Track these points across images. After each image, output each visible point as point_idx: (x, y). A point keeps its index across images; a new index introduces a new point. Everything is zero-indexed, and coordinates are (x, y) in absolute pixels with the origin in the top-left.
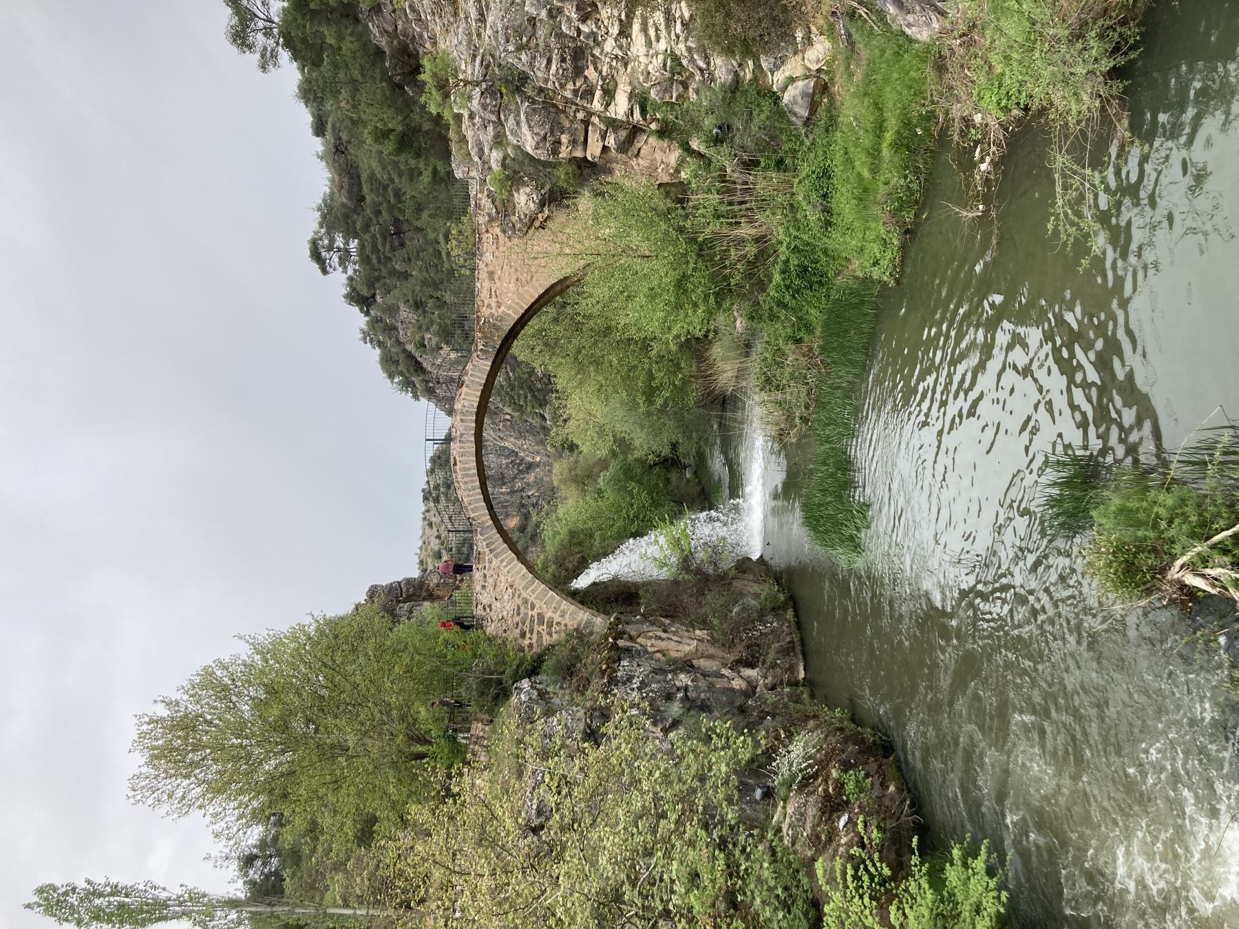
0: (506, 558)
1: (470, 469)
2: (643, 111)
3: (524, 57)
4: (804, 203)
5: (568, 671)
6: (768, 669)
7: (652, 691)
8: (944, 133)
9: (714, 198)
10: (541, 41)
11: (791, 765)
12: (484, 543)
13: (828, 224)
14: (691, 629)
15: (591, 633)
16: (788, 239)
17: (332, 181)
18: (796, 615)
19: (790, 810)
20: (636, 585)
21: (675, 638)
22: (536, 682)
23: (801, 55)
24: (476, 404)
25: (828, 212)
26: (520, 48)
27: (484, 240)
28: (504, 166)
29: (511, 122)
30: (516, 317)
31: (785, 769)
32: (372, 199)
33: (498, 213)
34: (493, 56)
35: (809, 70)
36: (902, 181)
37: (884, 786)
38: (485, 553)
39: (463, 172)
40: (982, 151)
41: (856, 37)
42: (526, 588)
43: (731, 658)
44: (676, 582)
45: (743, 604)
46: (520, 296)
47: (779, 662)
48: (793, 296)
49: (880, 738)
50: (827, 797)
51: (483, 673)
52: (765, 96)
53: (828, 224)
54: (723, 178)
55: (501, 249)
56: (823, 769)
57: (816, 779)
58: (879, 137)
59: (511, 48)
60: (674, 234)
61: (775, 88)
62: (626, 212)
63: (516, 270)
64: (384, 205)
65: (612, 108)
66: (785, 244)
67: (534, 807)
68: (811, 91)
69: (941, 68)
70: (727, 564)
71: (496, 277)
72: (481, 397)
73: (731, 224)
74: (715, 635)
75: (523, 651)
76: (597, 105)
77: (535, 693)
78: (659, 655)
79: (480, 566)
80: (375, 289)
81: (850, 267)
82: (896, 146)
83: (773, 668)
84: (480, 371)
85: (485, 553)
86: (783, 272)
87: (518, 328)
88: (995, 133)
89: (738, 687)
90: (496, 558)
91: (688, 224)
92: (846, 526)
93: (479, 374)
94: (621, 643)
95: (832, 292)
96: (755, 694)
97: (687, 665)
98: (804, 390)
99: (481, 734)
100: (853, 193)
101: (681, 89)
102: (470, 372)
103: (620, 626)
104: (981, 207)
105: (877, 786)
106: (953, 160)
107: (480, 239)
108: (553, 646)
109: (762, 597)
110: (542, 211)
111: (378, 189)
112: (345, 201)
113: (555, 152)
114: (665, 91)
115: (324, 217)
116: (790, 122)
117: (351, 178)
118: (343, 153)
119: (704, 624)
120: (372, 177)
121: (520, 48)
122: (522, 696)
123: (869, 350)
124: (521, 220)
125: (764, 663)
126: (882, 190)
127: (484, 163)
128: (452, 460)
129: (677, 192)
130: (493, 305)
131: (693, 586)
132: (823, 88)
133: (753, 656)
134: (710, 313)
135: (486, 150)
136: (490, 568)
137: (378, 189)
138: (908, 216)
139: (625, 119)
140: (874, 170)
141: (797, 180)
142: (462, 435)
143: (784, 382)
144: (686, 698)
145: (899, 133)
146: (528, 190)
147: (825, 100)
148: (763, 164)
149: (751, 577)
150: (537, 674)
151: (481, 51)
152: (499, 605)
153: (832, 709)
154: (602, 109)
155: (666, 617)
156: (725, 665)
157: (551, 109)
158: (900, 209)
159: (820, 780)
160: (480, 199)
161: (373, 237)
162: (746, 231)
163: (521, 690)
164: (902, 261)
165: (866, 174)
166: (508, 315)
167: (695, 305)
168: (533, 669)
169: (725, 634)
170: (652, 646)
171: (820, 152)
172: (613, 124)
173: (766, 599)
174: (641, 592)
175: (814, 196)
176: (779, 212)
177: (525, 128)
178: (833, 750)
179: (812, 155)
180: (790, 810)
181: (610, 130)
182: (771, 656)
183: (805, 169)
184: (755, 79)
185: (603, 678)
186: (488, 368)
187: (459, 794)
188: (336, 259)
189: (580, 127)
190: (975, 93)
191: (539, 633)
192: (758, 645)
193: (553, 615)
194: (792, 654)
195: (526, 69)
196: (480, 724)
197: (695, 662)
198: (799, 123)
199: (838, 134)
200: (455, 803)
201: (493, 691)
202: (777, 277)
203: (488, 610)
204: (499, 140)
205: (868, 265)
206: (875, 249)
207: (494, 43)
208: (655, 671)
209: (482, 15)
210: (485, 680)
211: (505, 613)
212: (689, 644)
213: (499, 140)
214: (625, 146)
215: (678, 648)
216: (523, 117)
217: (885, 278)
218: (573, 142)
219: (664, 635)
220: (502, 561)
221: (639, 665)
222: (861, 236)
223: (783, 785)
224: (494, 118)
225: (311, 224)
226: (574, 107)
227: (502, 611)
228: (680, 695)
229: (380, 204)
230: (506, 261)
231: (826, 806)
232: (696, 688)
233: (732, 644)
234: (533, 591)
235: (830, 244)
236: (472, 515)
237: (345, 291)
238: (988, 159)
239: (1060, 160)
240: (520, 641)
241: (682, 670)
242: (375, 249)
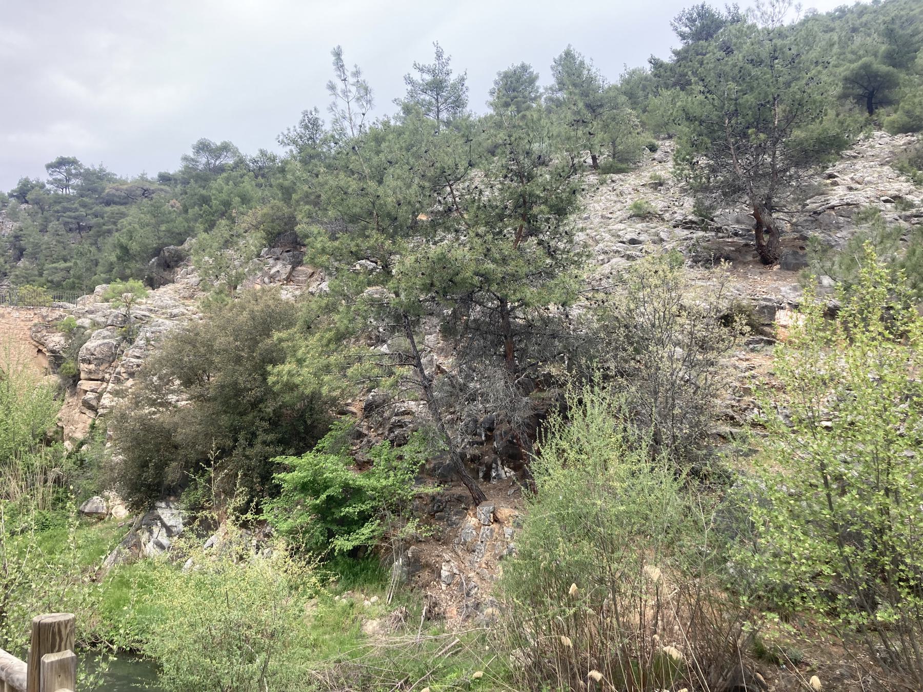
3: (142, 342)
10: (151, 352)
17: (124, 182)
26: (148, 340)
27: (30, 312)
28: (79, 327)
29: (105, 332)
32: (106, 212)
33: (49, 322)
34: (147, 322)
55: (22, 323)
59: (148, 335)
64: (102, 221)
80: (33, 204)
107: (29, 309)
110: (48, 351)
111: (114, 218)
112: (106, 191)
113: (84, 361)
115: (94, 173)
117: (125, 198)
118: (143, 194)
120: (123, 215)
121: (148, 340)
124: (43, 337)
127: (83, 314)
132: (101, 519)
135: (90, 316)
137: (114, 218)
139: (101, 404)
146: (63, 342)
151: (153, 315)
154: (108, 390)
157: (111, 358)
160: (59, 310)
161: (76, 210)
177: (100, 342)
181: (97, 395)
188: (59, 177)
189: (100, 377)
195: (136, 343)
204: (95, 325)
209: (174, 316)
213: (95, 325)
214: (88, 405)
216: (106, 341)
218: (90, 372)
224: (109, 322)
225: (89, 162)
229: (103, 218)
230: (12, 326)
237: (33, 179)
242: (66, 210)
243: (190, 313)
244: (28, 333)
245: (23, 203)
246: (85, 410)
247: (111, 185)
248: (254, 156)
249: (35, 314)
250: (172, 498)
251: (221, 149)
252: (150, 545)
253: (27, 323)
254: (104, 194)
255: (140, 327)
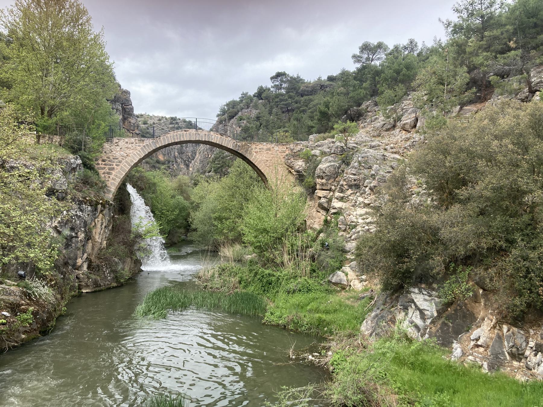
0: (141, 154)
1: (183, 137)
2: (334, 213)
3: (356, 164)
4: (297, 281)
5: (86, 182)
6: (87, 275)
7: (75, 221)
8: (325, 339)
9: (299, 243)
10: (362, 171)
11: (36, 288)
12: (148, 143)
13: (289, 292)
14: (106, 239)
15: (104, 192)
16: (282, 276)
17: (310, 83)
18: (114, 287)
19: (12, 288)
20: (129, 213)
21: (102, 232)
22: (80, 166)
23: (356, 278)
24: (213, 141)
25: (293, 292)
26: (360, 163)
27: (284, 147)
29: (330, 158)
30: (251, 160)
31: (34, 284)
32: (302, 100)
33: (294, 153)
35: (351, 282)
36: (305, 323)
37: (25, 332)
38: (144, 143)
39: (312, 139)
40: (317, 356)
41: (363, 301)
42: (126, 162)
43: (93, 258)
44: (130, 232)
45: (119, 263)
46: (260, 162)
47: (91, 280)
48: (259, 279)
49: (50, 329)
50: (19, 305)
51: (85, 142)
52: (340, 264)
53: (289, 292)
54: (307, 247)
56: (34, 303)
57: (29, 300)
58: (323, 312)
59: (360, 159)
60: (285, 227)
61: (343, 268)
62: (294, 207)
63: (271, 160)
65: (336, 200)
66: (280, 274)
67: (15, 165)
68: (342, 283)
69: (350, 336)
70: (139, 254)
71: (268, 151)
72: (216, 144)
73: (289, 251)
74: (104, 250)
75: (96, 161)
76: (337, 194)
77: (75, 166)
78: (93, 224)
79: (137, 141)
80: (264, 100)
81: (271, 303)
82: (320, 321)
83: (88, 277)
84: (228, 143)
85: (144, 143)
86: (269, 274)
87: (247, 161)
88: (324, 361)
89: (78, 261)
90: (141, 149)
91: (289, 233)
92: (155, 308)
93: (226, 143)
94: (99, 206)
95: (260, 296)
96: (75, 269)
97: (89, 237)
98: (218, 286)
99: (54, 140)
100: (301, 302)
101: (343, 229)
102: (227, 139)
103: (108, 206)
104: (294, 357)
105: (24, 329)
106: (313, 344)
107: (284, 145)
108: (98, 175)
109: (122, 272)
111: (306, 103)
113: (319, 177)
114: (342, 222)
115: (295, 79)
116: (330, 274)
118: (321, 88)
119: (109, 245)
120: (311, 100)
122: (73, 160)
123: (234, 314)
124: (292, 162)
125: (90, 273)
126: (302, 315)
127: (315, 147)
128: (187, 130)
129: (301, 229)
130: (256, 150)
131: (128, 240)
133: (93, 268)
134: (252, 244)
135: (319, 148)
136: (136, 146)
137: (306, 103)
138: (291, 327)
139: (332, 206)
140: (310, 311)
141: (306, 278)
142: (199, 134)
143: (222, 277)
144: (72, 237)
145: (325, 321)
146: (304, 165)
147: (339, 289)
148: (313, 264)
149: (132, 266)
150: (84, 167)
151: (359, 147)
152: (118, 149)
153: (66, 306)
154: (336, 196)
155: (113, 227)
156: (89, 255)
157: (335, 175)
158: (294, 323)
159: (29, 302)
161: (287, 100)
162: (286, 257)
163: (76, 160)
164: (273, 325)
165: (309, 308)
166: (252, 157)
167: (256, 237)
168: (87, 165)
169: (104, 255)
170: (98, 221)
171: (318, 287)
172: (330, 201)
173: (121, 273)
174: (125, 216)
175: (300, 286)
176: (294, 271)
177: (328, 164)
178: (44, 307)
179: (316, 284)
180: (12, 288)
182: (93, 277)
183: (311, 281)
184: (347, 259)
185: (82, 198)
186: (229, 147)
187: (19, 128)
188: (277, 83)
189: (329, 188)
190: (340, 351)
191: (105, 168)
192: (99, 270)
193: (113, 175)
194: (94, 286)
196: (59, 140)
197: (90, 241)
198: (330, 278)
199: (324, 295)
200: (15, 126)
201: (76, 146)
202: (267, 272)
203: (116, 144)
204: (323, 154)
205: (271, 310)
206: (278, 313)
207: (362, 152)
208: (85, 223)
209: (373, 147)
210: (82, 143)
211: (114, 152)
212: (99, 238)
213: (323, 154)
214: (321, 206)
215: (97, 233)
216: (332, 164)
217: (265, 318)
218: (322, 185)
219: (103, 226)
220: (139, 151)
221: (88, 215)
222: (283, 307)
223: (26, 284)
224: (332, 151)
225: (292, 72)
226: (336, 185)
227: (115, 151)
228: (73, 234)
229: (300, 103)
231: (14, 305)
232: (78, 242)
233: (99, 258)
234: (125, 166)
235: (280, 294)
236: (161, 138)
238: (313, 358)
239: (311, 388)
240: (101, 159)
241: (86, 235)
242: (281, 100)
243: (384, 145)
244: (283, 160)
245: (260, 100)
246: (320, 210)
247: (304, 85)
248: (405, 44)
249: (287, 148)
250: (423, 286)
251: (377, 47)
252: (406, 323)
253: (283, 154)
254: (300, 90)
255: (353, 154)
